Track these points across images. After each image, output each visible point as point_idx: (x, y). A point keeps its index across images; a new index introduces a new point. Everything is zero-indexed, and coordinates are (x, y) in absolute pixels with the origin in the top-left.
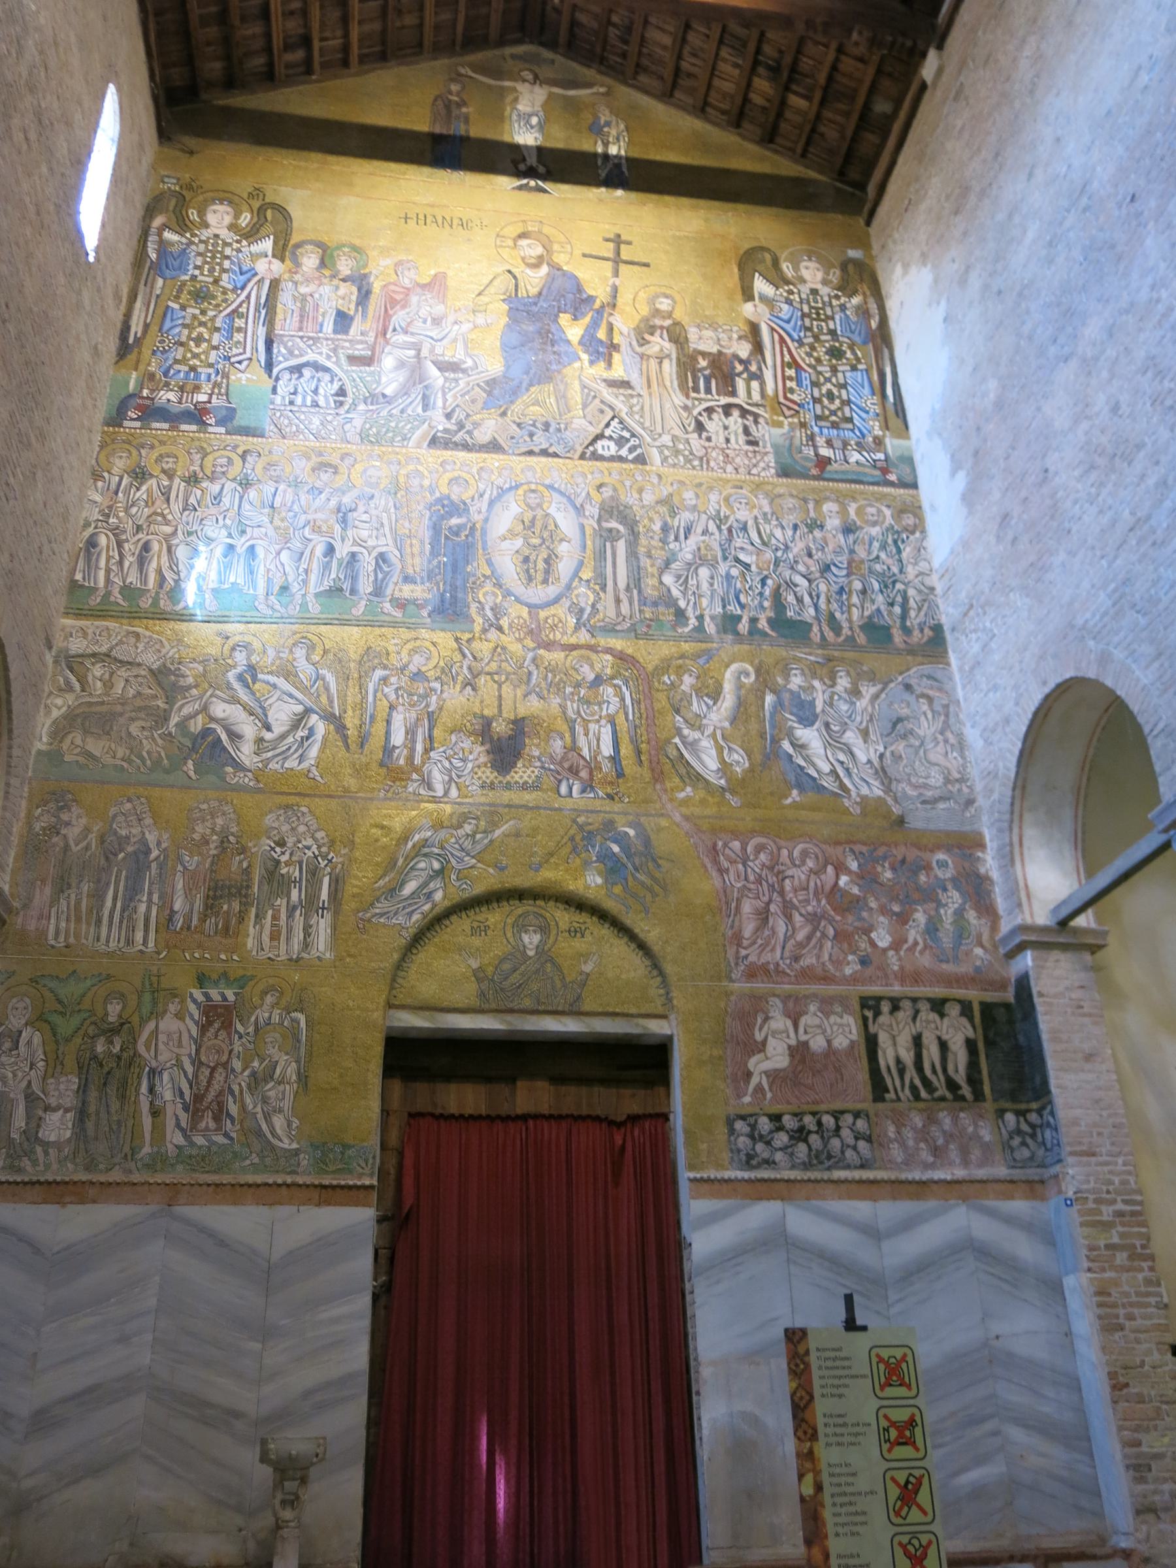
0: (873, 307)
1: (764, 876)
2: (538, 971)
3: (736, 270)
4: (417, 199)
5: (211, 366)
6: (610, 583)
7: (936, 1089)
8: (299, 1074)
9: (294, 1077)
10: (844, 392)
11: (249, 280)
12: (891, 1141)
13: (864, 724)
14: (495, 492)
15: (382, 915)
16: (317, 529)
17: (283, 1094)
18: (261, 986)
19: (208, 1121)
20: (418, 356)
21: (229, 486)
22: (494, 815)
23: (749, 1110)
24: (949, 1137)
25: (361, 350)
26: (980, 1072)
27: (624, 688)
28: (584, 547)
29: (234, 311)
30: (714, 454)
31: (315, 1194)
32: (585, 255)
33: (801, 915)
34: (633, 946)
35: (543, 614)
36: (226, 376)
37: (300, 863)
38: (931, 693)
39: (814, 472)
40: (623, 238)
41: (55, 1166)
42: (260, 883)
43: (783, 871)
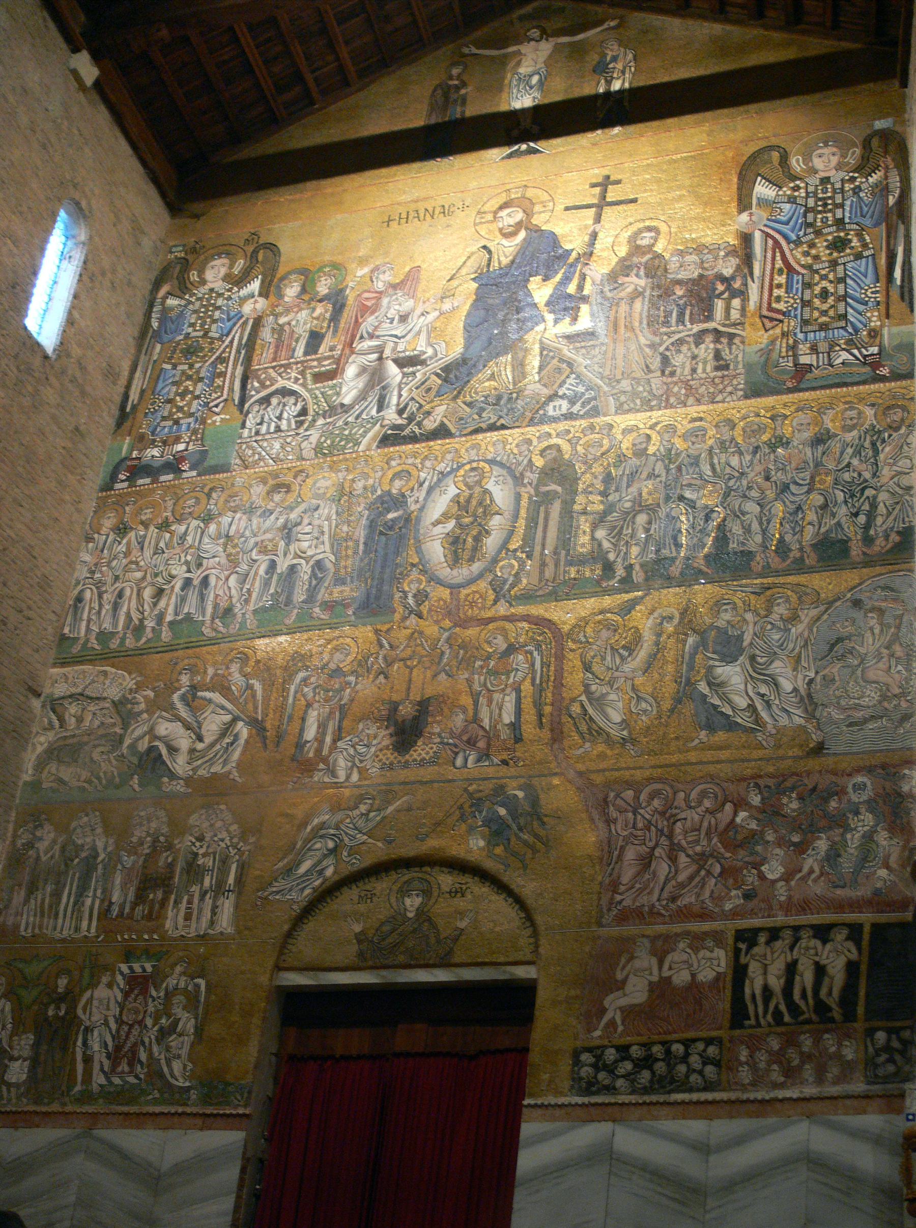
0: (895, 180)
1: (653, 822)
2: (414, 931)
3: (735, 180)
4: (403, 198)
5: (191, 415)
6: (538, 548)
7: (803, 1013)
8: (196, 1027)
9: (192, 1030)
10: (841, 287)
11: (235, 325)
12: (741, 1064)
13: (796, 651)
14: (435, 479)
15: (277, 893)
16: (264, 551)
17: (182, 1044)
18: (172, 960)
19: (124, 1067)
20: (380, 359)
21: (195, 523)
22: (388, 794)
23: (598, 1043)
24: (806, 1058)
25: (327, 366)
26: (856, 994)
27: (535, 653)
28: (516, 516)
29: (219, 358)
30: (676, 389)
31: (199, 1121)
32: (567, 209)
33: (688, 856)
34: (510, 900)
35: (464, 592)
36: (203, 422)
37: (214, 853)
38: (883, 605)
39: (789, 385)
40: (612, 178)
41: (14, 1101)
42: (181, 873)
43: (675, 815)
